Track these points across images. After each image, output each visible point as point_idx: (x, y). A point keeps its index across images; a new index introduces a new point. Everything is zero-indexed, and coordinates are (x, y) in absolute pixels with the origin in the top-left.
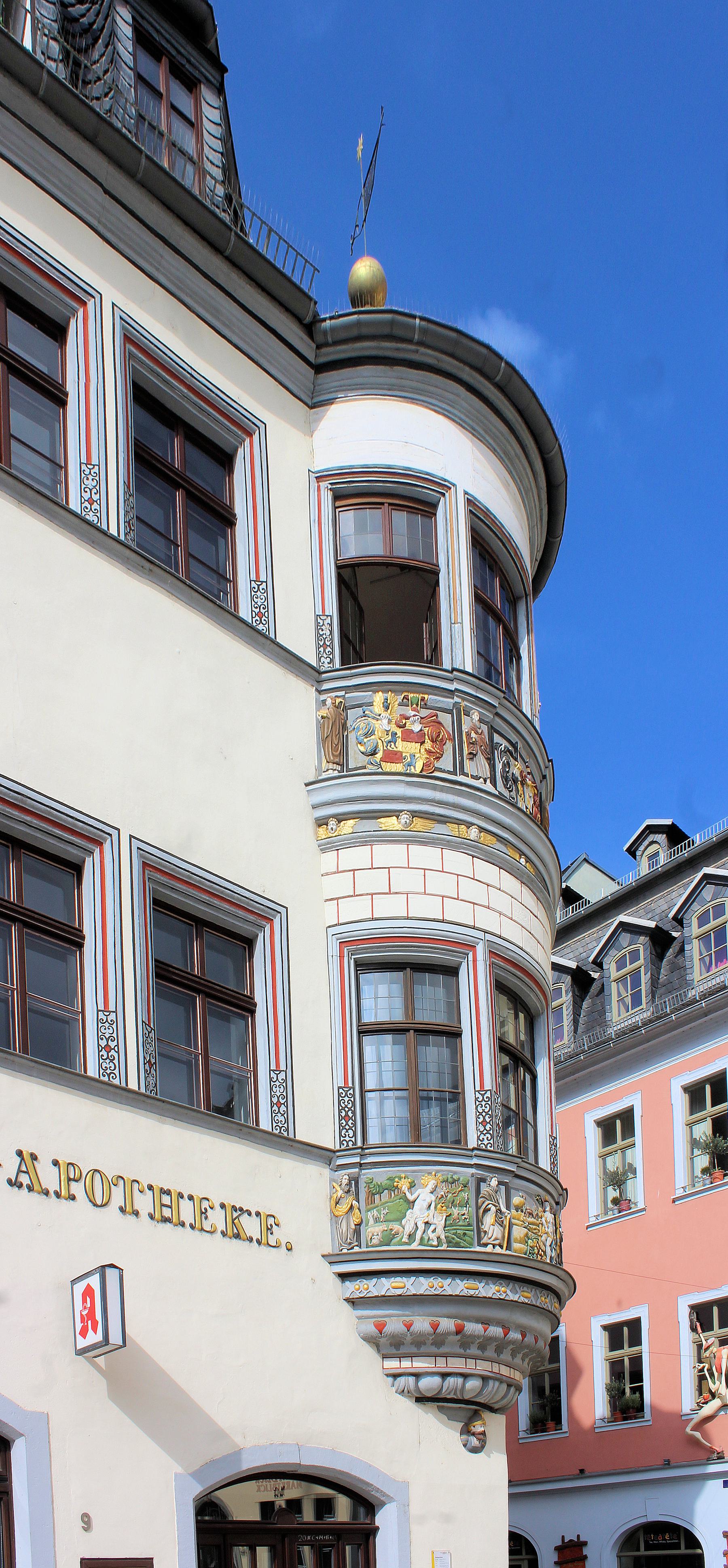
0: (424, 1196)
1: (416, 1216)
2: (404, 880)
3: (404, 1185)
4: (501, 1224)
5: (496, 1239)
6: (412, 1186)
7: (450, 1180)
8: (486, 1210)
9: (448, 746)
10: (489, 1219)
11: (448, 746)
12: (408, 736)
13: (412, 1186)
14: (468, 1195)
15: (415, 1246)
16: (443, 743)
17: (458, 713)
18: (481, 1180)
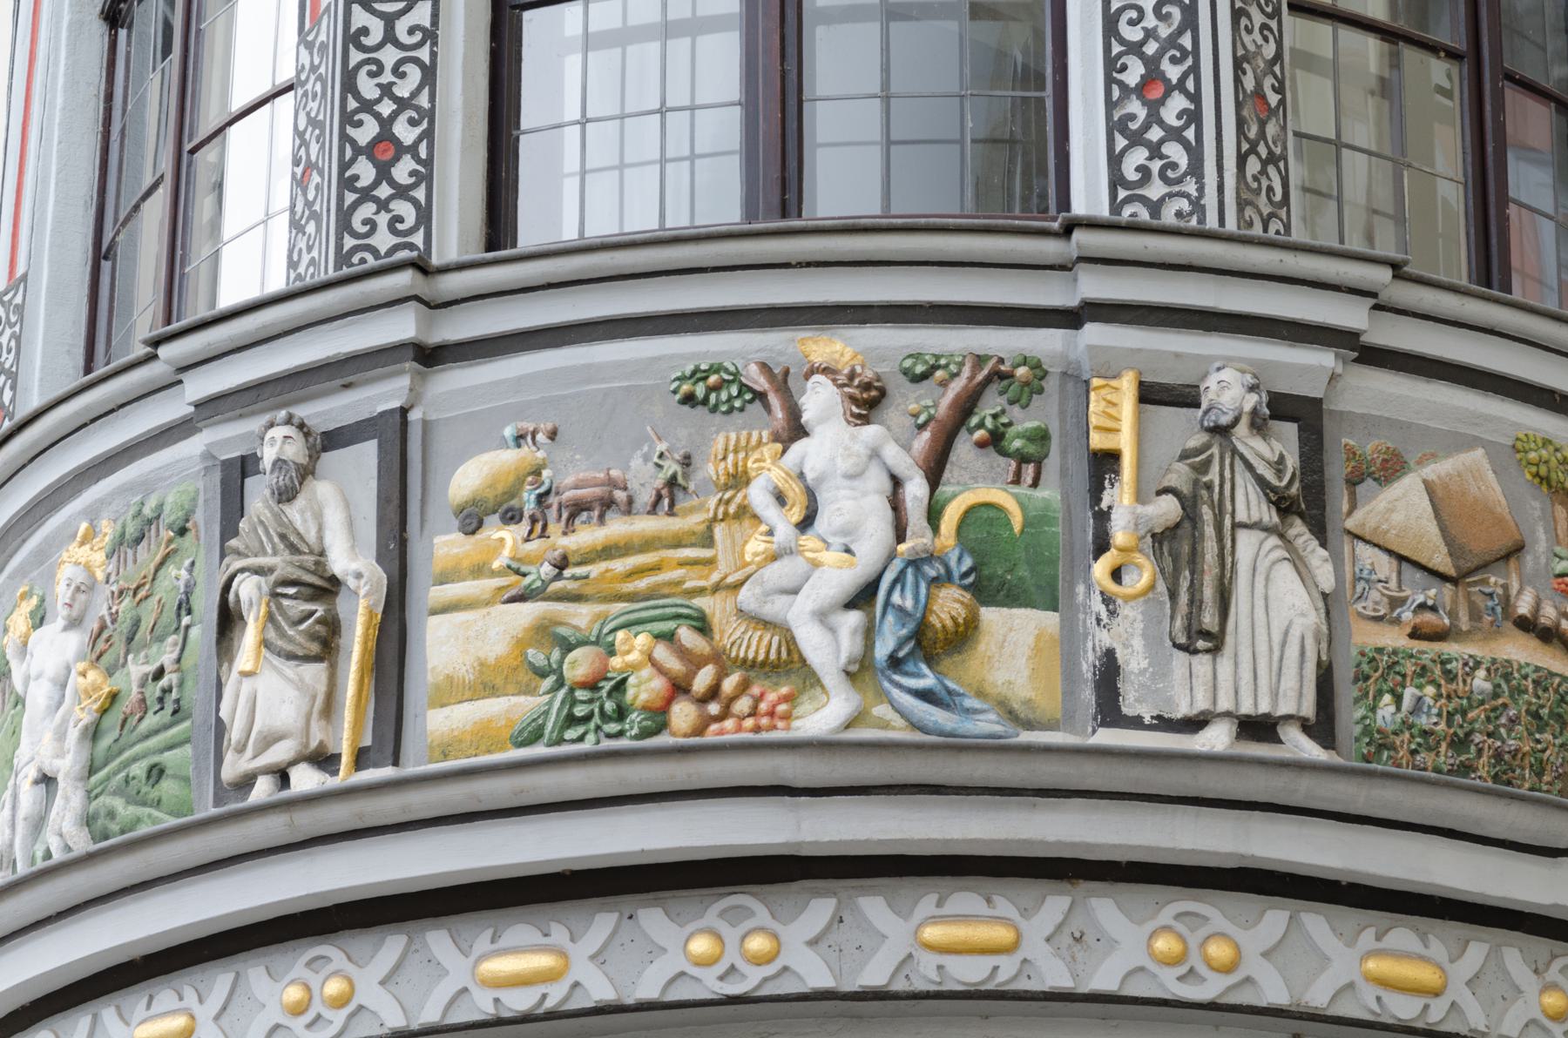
5: (269, 740)
7: (131, 530)
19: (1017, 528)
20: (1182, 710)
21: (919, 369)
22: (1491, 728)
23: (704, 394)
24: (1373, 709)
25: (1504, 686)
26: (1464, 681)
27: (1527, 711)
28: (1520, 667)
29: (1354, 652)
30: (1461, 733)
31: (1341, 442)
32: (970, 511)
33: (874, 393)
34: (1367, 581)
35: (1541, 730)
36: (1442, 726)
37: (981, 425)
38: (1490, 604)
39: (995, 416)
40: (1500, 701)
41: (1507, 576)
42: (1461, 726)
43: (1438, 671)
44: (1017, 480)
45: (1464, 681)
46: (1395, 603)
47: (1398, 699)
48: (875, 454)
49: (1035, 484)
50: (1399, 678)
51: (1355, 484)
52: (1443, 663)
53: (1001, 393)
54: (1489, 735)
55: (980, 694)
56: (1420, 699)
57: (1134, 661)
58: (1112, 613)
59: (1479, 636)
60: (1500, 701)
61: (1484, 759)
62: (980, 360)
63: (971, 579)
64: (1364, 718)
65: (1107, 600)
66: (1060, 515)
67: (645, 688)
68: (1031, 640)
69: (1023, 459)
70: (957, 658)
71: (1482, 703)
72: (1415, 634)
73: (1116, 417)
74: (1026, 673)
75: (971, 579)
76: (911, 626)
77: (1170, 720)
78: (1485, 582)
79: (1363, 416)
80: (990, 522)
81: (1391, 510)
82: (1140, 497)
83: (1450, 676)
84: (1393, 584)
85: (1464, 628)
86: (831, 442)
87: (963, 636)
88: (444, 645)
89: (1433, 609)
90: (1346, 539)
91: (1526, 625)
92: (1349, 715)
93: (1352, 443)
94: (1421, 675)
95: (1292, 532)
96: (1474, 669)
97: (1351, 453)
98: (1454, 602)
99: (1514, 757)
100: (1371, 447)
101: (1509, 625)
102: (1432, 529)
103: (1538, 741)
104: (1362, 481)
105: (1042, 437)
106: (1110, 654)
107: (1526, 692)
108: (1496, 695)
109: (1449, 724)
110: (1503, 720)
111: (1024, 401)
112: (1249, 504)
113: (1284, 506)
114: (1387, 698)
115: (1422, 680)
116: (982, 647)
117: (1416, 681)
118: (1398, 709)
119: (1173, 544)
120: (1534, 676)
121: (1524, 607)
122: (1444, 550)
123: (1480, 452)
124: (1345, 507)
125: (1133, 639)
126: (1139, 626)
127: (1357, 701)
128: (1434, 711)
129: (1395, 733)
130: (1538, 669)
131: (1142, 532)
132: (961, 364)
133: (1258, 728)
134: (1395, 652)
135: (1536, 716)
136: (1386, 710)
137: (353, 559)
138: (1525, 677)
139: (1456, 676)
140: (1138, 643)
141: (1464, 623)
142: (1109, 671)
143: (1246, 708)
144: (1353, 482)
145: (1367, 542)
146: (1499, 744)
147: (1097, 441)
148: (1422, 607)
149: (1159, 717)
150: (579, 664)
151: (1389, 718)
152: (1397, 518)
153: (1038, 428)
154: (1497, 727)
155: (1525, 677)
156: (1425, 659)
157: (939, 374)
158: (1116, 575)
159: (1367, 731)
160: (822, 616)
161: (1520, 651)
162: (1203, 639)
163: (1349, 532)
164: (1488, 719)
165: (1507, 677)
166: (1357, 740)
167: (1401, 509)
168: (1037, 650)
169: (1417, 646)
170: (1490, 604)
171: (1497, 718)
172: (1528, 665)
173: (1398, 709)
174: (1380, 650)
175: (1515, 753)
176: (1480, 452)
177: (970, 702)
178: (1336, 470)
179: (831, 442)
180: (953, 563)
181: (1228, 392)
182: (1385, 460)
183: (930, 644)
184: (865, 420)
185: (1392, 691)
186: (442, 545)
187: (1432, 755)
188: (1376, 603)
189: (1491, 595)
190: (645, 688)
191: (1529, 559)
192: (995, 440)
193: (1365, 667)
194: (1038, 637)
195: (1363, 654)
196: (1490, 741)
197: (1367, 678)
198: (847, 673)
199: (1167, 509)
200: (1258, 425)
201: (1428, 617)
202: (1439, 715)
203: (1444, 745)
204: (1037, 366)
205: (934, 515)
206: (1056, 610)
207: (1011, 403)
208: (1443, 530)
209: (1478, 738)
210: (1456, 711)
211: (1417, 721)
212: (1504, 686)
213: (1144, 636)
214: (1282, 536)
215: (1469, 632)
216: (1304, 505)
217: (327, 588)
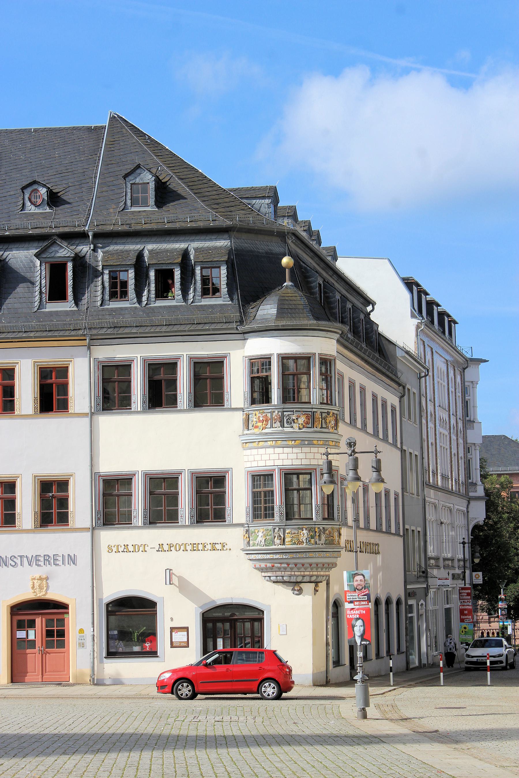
0: (260, 534)
1: (259, 539)
2: (258, 458)
3: (256, 531)
4: (280, 539)
6: (258, 531)
8: (275, 537)
9: (270, 421)
10: (276, 538)
11: (269, 421)
12: (260, 421)
13: (258, 531)
14: (272, 532)
15: (259, 547)
16: (268, 421)
17: (272, 413)
18: (274, 529)
23: (299, 528)
67: (297, 543)
73: (317, 530)
86: (305, 531)
88: (286, 540)
119: (319, 536)
137: (282, 536)
150: (293, 541)
162: (320, 540)
167: (327, 532)
179: (305, 531)
181: (321, 528)
183: (309, 541)
186: (286, 535)
190: (297, 543)
217: (280, 536)
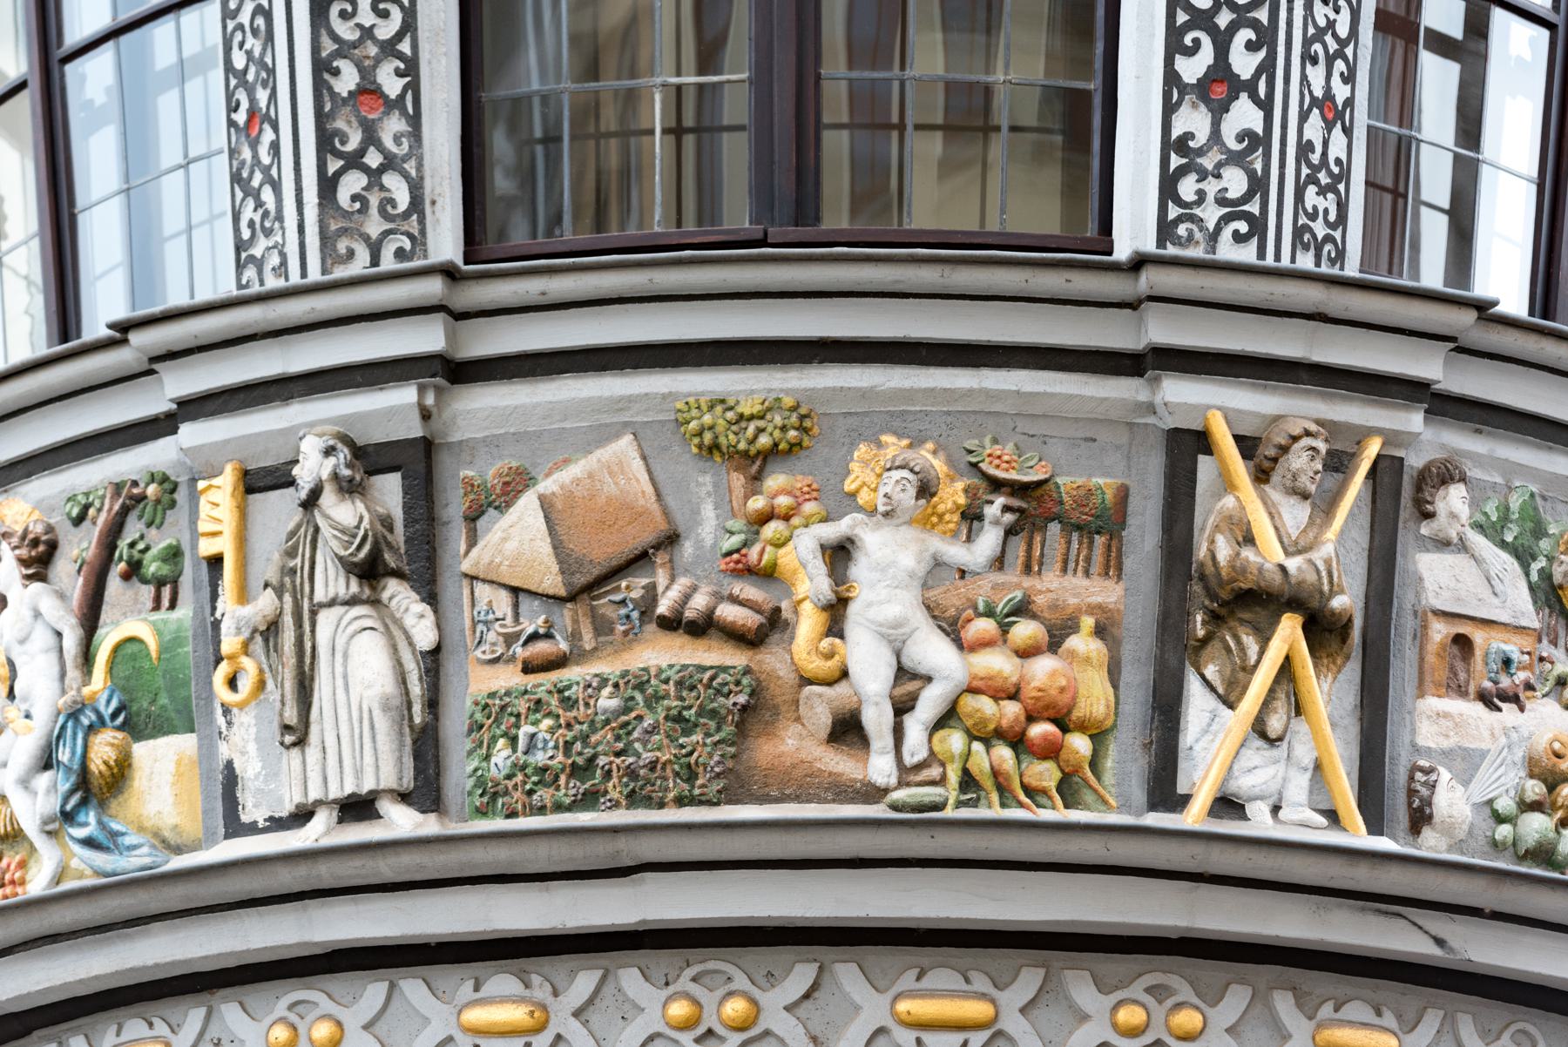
19: (154, 655)
20: (285, 810)
21: (75, 512)
22: (620, 745)
24: (487, 758)
25: (639, 697)
26: (587, 705)
27: (666, 718)
28: (660, 671)
29: (469, 702)
30: (580, 761)
31: (459, 477)
32: (117, 649)
33: (41, 548)
34: (486, 623)
35: (687, 733)
36: (560, 757)
37: (121, 559)
38: (623, 611)
39: (132, 545)
40: (633, 715)
41: (654, 573)
42: (580, 754)
43: (554, 701)
44: (157, 606)
45: (587, 705)
46: (510, 639)
47: (514, 740)
48: (37, 615)
49: (172, 606)
50: (513, 719)
51: (474, 520)
52: (560, 691)
53: (140, 517)
54: (618, 754)
55: (141, 829)
56: (533, 736)
57: (249, 769)
58: (229, 723)
59: (610, 649)
60: (633, 715)
61: (615, 780)
62: (118, 488)
63: (121, 719)
64: (476, 770)
65: (227, 711)
66: (190, 634)
68: (172, 767)
69: (160, 583)
70: (121, 799)
71: (607, 722)
72: (528, 668)
74: (171, 800)
75: (121, 719)
76: (73, 779)
77: (281, 819)
78: (618, 589)
79: (484, 439)
80: (134, 657)
81: (504, 540)
82: (243, 596)
83: (569, 703)
84: (509, 620)
85: (588, 647)
87: (120, 773)
89: (548, 636)
90: (465, 582)
91: (671, 624)
92: (459, 771)
93: (470, 473)
94: (536, 711)
95: (385, 596)
96: (599, 689)
97: (469, 484)
98: (575, 621)
99: (653, 769)
100: (490, 471)
101: (652, 627)
102: (545, 548)
103: (682, 747)
104: (483, 513)
105: (174, 555)
106: (229, 765)
107: (666, 696)
108: (626, 710)
109: (567, 753)
110: (636, 735)
111: (158, 521)
112: (330, 581)
113: (369, 571)
114: (501, 742)
115: (538, 716)
116: (136, 784)
117: (532, 717)
118: (515, 750)
120: (677, 677)
121: (663, 608)
122: (555, 568)
123: (625, 443)
124: (463, 548)
125: (247, 742)
126: (253, 730)
127: (470, 753)
128: (551, 744)
129: (509, 777)
130: (685, 667)
131: (246, 634)
132: (103, 497)
133: (358, 808)
134: (508, 693)
135: (679, 719)
136: (502, 756)
138: (666, 681)
139: (577, 701)
140: (252, 748)
141: (588, 641)
142: (231, 779)
143: (335, 793)
144: (472, 518)
145: (484, 581)
146: (631, 760)
147: (207, 548)
148: (534, 637)
149: (271, 819)
151: (501, 765)
152: (511, 546)
153: (170, 547)
154: (630, 743)
155: (666, 681)
156: (541, 693)
157: (92, 512)
158: (232, 683)
159: (481, 782)
160: (25, 783)
161: (661, 654)
163: (466, 575)
164: (618, 738)
165: (640, 686)
166: (470, 794)
167: (517, 540)
168: (179, 775)
169: (532, 680)
170: (623, 611)
171: (629, 733)
172: (671, 666)
173: (515, 750)
174: (492, 695)
175: (652, 766)
176: (625, 443)
177: (128, 840)
178: (453, 506)
180: (102, 708)
182: (506, 484)
184: (40, 577)
185: (505, 735)
187: (551, 790)
188: (494, 644)
189: (623, 602)
191: (687, 549)
192: (134, 571)
193: (479, 716)
194: (178, 763)
195: (476, 703)
196: (618, 761)
197: (481, 727)
198: (49, 833)
199: (265, 603)
200: (349, 488)
201: (542, 647)
202: (556, 747)
203: (563, 780)
204: (165, 479)
205: (87, 658)
206: (192, 731)
207: (149, 525)
208: (557, 546)
209: (602, 760)
210: (575, 739)
211: (531, 760)
212: (639, 697)
213: (257, 740)
214: (375, 602)
215: (595, 649)
216: (401, 560)
